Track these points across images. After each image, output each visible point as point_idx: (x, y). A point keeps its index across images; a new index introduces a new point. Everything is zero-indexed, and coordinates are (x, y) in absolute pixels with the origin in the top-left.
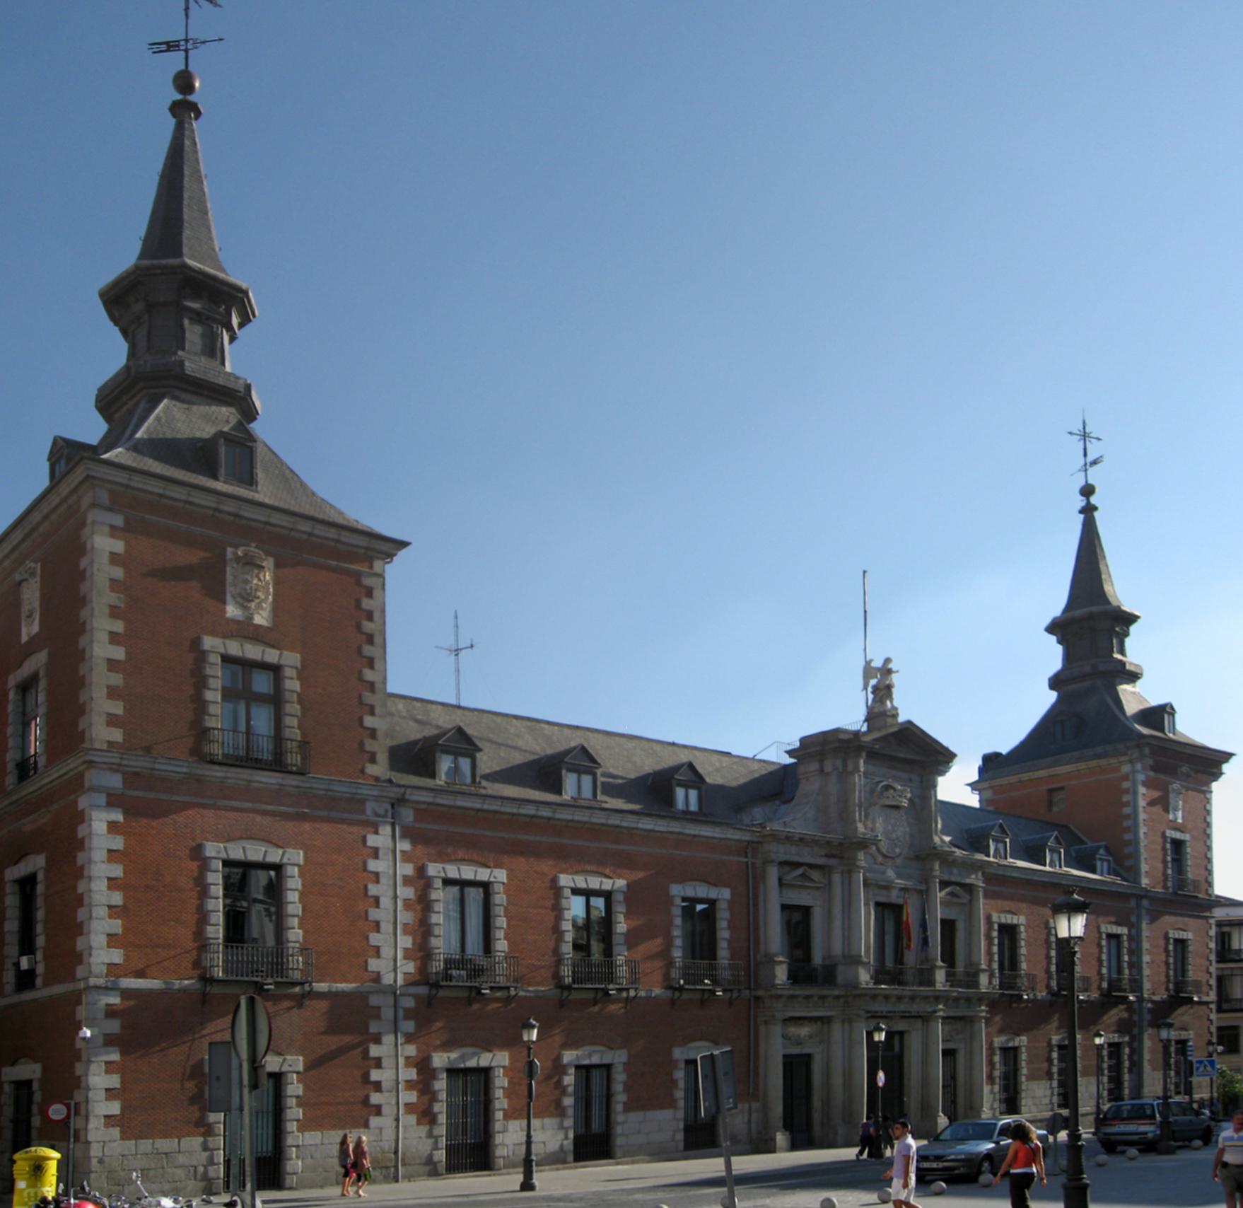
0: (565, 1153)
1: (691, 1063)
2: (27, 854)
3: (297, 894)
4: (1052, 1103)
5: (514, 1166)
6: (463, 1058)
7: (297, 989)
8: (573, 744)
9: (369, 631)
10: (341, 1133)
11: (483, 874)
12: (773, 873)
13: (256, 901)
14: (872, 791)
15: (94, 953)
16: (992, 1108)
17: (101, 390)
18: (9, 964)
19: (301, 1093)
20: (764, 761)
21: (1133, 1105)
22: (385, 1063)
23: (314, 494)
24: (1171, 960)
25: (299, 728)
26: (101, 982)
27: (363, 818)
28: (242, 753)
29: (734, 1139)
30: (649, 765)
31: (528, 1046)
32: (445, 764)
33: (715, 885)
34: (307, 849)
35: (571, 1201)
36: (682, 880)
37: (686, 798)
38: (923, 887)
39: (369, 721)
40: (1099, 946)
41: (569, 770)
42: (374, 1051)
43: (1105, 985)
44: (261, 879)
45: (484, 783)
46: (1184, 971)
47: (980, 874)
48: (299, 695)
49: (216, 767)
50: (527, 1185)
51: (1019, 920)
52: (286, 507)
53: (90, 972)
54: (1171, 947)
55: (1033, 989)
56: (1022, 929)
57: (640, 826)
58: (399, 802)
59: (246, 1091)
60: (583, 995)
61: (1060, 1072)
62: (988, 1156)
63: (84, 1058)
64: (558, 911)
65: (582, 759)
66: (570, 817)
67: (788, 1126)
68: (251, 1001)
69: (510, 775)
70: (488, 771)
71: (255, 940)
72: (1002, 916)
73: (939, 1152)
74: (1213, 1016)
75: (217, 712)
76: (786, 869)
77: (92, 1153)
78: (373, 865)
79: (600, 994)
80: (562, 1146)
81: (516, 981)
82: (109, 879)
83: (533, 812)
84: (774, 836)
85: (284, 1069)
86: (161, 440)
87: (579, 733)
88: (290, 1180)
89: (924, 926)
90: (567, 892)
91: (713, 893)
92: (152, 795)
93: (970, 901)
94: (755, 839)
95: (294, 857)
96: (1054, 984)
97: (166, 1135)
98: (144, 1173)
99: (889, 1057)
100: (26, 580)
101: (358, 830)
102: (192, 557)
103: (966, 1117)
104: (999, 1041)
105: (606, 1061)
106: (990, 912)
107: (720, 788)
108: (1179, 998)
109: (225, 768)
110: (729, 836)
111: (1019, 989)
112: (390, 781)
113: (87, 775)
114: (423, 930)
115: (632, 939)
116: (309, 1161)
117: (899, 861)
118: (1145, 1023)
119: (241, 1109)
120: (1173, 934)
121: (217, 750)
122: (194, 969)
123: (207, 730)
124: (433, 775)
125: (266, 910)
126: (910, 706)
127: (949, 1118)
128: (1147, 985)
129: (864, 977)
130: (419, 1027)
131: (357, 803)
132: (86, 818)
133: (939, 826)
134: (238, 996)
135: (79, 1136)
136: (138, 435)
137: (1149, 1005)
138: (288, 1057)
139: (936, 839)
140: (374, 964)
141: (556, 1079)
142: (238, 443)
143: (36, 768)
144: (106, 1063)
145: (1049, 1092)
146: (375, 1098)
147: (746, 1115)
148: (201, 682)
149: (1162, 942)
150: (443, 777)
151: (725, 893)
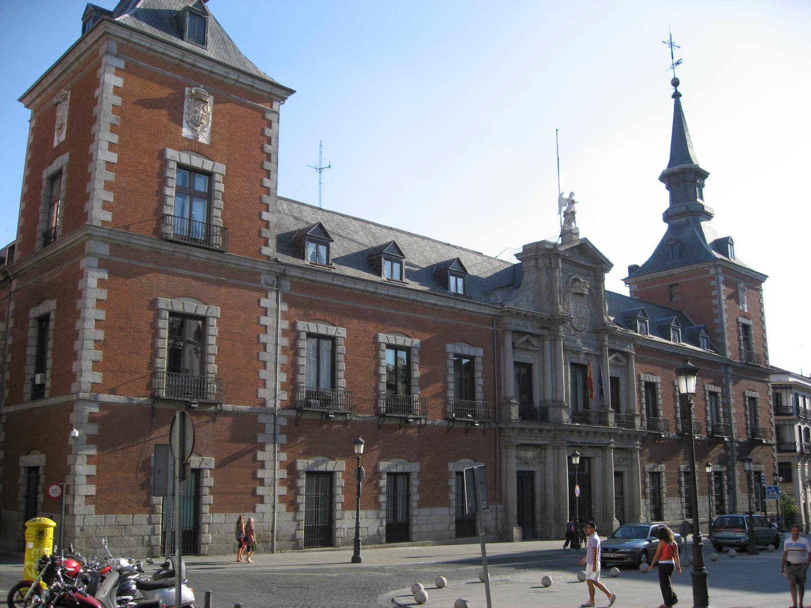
0: (380, 536)
1: (460, 474)
2: (45, 299)
3: (215, 338)
4: (682, 514)
5: (348, 544)
6: (317, 464)
7: (212, 408)
8: (389, 240)
9: (269, 152)
10: (237, 515)
11: (332, 331)
12: (509, 338)
13: (189, 342)
14: (567, 282)
15: (84, 374)
16: (646, 516)
18: (28, 380)
19: (212, 485)
20: (502, 261)
21: (731, 518)
22: (267, 465)
23: (240, 53)
24: (748, 412)
25: (222, 218)
26: (86, 395)
27: (259, 286)
28: (186, 234)
29: (487, 531)
30: (434, 258)
31: (358, 457)
32: (310, 249)
34: (223, 306)
35: (384, 572)
36: (453, 342)
37: (456, 284)
38: (599, 353)
39: (265, 216)
40: (705, 400)
41: (386, 259)
42: (261, 456)
43: (710, 429)
44: (193, 325)
45: (334, 265)
46: (756, 421)
47: (632, 344)
48: (223, 193)
49: (168, 244)
50: (356, 559)
51: (657, 379)
52: (223, 61)
53: (80, 388)
54: (747, 403)
55: (668, 430)
56: (659, 386)
57: (429, 301)
58: (281, 276)
59: (177, 481)
61: (687, 491)
62: (645, 550)
63: (73, 452)
64: (377, 359)
65: (394, 252)
66: (386, 293)
67: (521, 523)
68: (183, 415)
70: (337, 256)
71: (187, 370)
72: (647, 375)
73: (615, 546)
74: (775, 455)
75: (172, 204)
76: (517, 336)
77: (76, 524)
78: (264, 320)
79: (403, 422)
81: (351, 409)
82: (97, 321)
83: (363, 288)
84: (509, 312)
85: (202, 466)
86: (151, 10)
87: (392, 232)
88: (204, 549)
89: (600, 381)
90: (383, 346)
91: (472, 352)
92: (126, 261)
93: (627, 364)
94: (498, 314)
95: (215, 311)
96: (680, 427)
97: (125, 512)
100: (60, 103)
101: (255, 294)
102: (161, 92)
104: (648, 467)
105: (407, 470)
106: (641, 373)
107: (476, 278)
108: (754, 442)
109: (174, 245)
110: (482, 311)
111: (659, 430)
112: (276, 260)
113: (87, 244)
114: (293, 369)
115: (424, 382)
116: (216, 535)
117: (584, 333)
118: (735, 458)
119: (174, 495)
120: (749, 394)
121: (170, 231)
123: (164, 216)
124: (302, 257)
125: (195, 349)
126: (585, 230)
128: (735, 430)
129: (566, 417)
130: (289, 440)
131: (255, 275)
132: (85, 275)
133: (607, 309)
134: (174, 411)
135: (68, 510)
136: (138, 6)
137: (737, 445)
138: (205, 458)
139: (605, 318)
140: (262, 393)
141: (375, 481)
142: (197, 15)
143: (55, 237)
144: (88, 456)
145: (680, 506)
146: (260, 491)
147: (495, 513)
148: (163, 181)
149: (742, 399)
150: (309, 259)
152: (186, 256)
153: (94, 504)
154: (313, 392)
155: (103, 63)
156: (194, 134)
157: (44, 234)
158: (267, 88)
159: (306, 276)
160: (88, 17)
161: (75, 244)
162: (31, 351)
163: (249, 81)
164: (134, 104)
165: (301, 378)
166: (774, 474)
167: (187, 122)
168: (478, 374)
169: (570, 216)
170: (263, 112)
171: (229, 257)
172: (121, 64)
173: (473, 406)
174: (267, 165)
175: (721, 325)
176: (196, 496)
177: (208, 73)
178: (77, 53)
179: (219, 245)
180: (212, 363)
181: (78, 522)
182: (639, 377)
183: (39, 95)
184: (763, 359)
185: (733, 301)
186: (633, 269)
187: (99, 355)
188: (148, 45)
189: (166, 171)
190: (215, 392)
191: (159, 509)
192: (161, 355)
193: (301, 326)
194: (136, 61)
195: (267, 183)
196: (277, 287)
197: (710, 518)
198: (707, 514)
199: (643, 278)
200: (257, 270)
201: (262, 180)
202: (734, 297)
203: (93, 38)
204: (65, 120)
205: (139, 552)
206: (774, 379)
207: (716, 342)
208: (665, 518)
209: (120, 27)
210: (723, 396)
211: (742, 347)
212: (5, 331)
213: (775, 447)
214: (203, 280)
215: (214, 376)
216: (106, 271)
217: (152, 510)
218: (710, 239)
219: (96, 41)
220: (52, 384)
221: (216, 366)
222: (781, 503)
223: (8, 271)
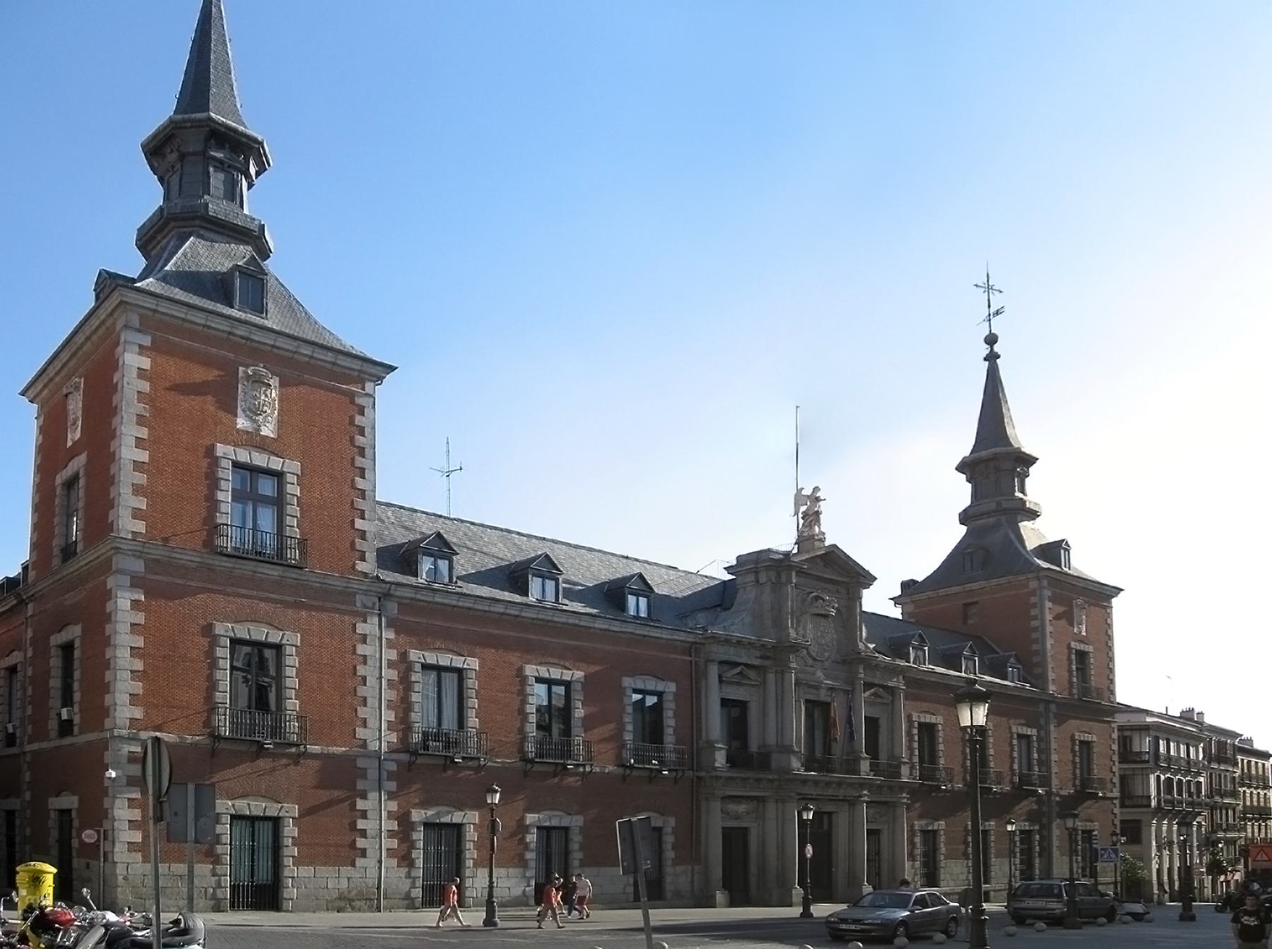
6: (438, 815)
7: (293, 750)
11: (458, 662)
12: (714, 671)
14: (804, 601)
18: (53, 714)
22: (369, 815)
24: (1077, 760)
32: (426, 565)
36: (632, 674)
39: (359, 524)
40: (1011, 745)
41: (534, 575)
42: (360, 804)
45: (460, 583)
46: (1090, 770)
51: (936, 719)
54: (1077, 748)
56: (940, 727)
62: (903, 922)
64: (523, 696)
65: (548, 567)
66: (534, 616)
67: (727, 885)
69: (481, 578)
74: (1117, 811)
76: (726, 667)
79: (559, 768)
83: (502, 610)
84: (714, 638)
92: (170, 579)
99: (820, 832)
103: (889, 888)
104: (918, 825)
106: (910, 713)
108: (1084, 793)
109: (233, 560)
112: (378, 577)
115: (588, 723)
118: (1054, 815)
123: (217, 526)
127: (874, 888)
128: (1055, 782)
129: (796, 764)
130: (401, 787)
131: (347, 596)
139: (861, 646)
140: (361, 733)
145: (965, 870)
146: (361, 843)
148: (213, 483)
149: (1069, 744)
151: (671, 687)
158: (356, 365)
159: (419, 597)
162: (55, 683)
163: (330, 357)
165: (415, 717)
166: (1114, 834)
167: (244, 411)
169: (812, 517)
170: (351, 396)
172: (147, 341)
173: (662, 750)
174: (359, 461)
175: (1043, 652)
178: (87, 330)
182: (909, 717)
184: (1106, 693)
185: (1063, 622)
186: (908, 586)
188: (183, 316)
194: (166, 336)
197: (1010, 885)
198: (1006, 881)
199: (923, 596)
201: (353, 481)
202: (1068, 617)
206: (1121, 719)
207: (1032, 669)
208: (942, 883)
210: (1040, 739)
211: (1075, 680)
213: (1117, 802)
214: (275, 601)
218: (1031, 544)
219: (111, 314)
222: (1120, 867)
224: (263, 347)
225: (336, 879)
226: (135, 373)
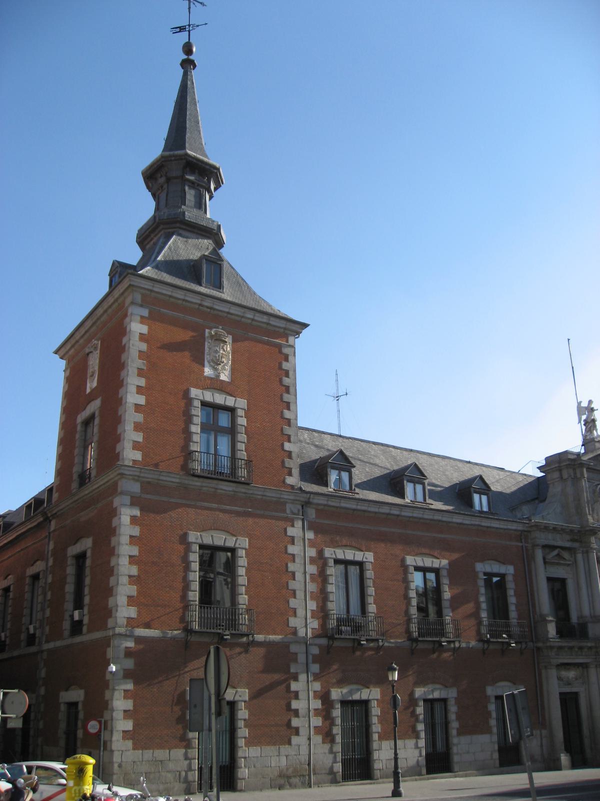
1: (499, 698)
2: (81, 537)
3: (244, 569)
5: (387, 777)
6: (351, 693)
7: (245, 639)
8: (409, 462)
9: (287, 385)
11: (359, 556)
12: (539, 554)
15: (119, 609)
17: (139, 231)
18: (67, 616)
19: (247, 717)
20: (525, 475)
22: (301, 695)
23: (255, 293)
26: (122, 630)
28: (212, 468)
29: (532, 759)
30: (456, 477)
31: (392, 684)
32: (333, 476)
33: (504, 563)
36: (482, 560)
37: (480, 502)
39: (287, 446)
41: (408, 481)
42: (294, 686)
44: (222, 557)
45: (357, 490)
48: (245, 427)
49: (196, 479)
50: (396, 793)
52: (240, 302)
53: (116, 623)
57: (454, 520)
60: (426, 646)
63: (111, 687)
64: (406, 582)
65: (415, 474)
66: (410, 515)
67: (568, 750)
69: (372, 484)
70: (359, 481)
71: (219, 602)
75: (198, 442)
77: (115, 760)
78: (291, 549)
79: (437, 645)
80: (418, 761)
81: (383, 635)
82: (130, 557)
84: (537, 526)
86: (171, 261)
87: (412, 454)
88: (241, 784)
90: (411, 569)
94: (526, 529)
95: (244, 542)
97: (161, 747)
98: (147, 775)
100: (91, 352)
101: (281, 524)
105: (442, 696)
107: (500, 494)
109: (201, 480)
110: (509, 527)
112: (300, 489)
113: (120, 484)
114: (323, 597)
115: (456, 602)
119: (210, 730)
121: (196, 467)
122: (180, 623)
124: (326, 484)
125: (225, 580)
130: (322, 669)
131: (280, 505)
135: (106, 745)
136: (159, 259)
138: (239, 690)
140: (293, 622)
141: (412, 709)
143: (90, 478)
144: (125, 691)
146: (295, 722)
148: (188, 419)
152: (213, 490)
153: (131, 739)
154: (343, 619)
155: (129, 314)
156: (216, 373)
157: (79, 475)
158: (282, 324)
160: (114, 272)
161: (108, 484)
162: (70, 588)
163: (265, 319)
164: (158, 347)
167: (209, 362)
168: (511, 592)
170: (279, 347)
171: (255, 489)
172: (145, 312)
173: (508, 625)
174: (286, 397)
176: (231, 729)
177: (226, 315)
179: (244, 477)
180: (242, 594)
181: (117, 758)
183: (73, 346)
187: (133, 590)
188: (170, 293)
189: (191, 409)
190: (247, 623)
191: (195, 743)
192: (193, 588)
193: (328, 552)
194: (159, 308)
195: (287, 414)
196: (303, 516)
200: (282, 500)
201: (282, 412)
203: (119, 291)
204: (97, 368)
205: (176, 789)
209: (142, 279)
212: (45, 569)
215: (245, 607)
216: (138, 508)
217: (188, 746)
219: (123, 294)
220: (90, 619)
221: (246, 596)
223: (48, 512)
224: (220, 313)
225: (276, 758)
226: (137, 338)
